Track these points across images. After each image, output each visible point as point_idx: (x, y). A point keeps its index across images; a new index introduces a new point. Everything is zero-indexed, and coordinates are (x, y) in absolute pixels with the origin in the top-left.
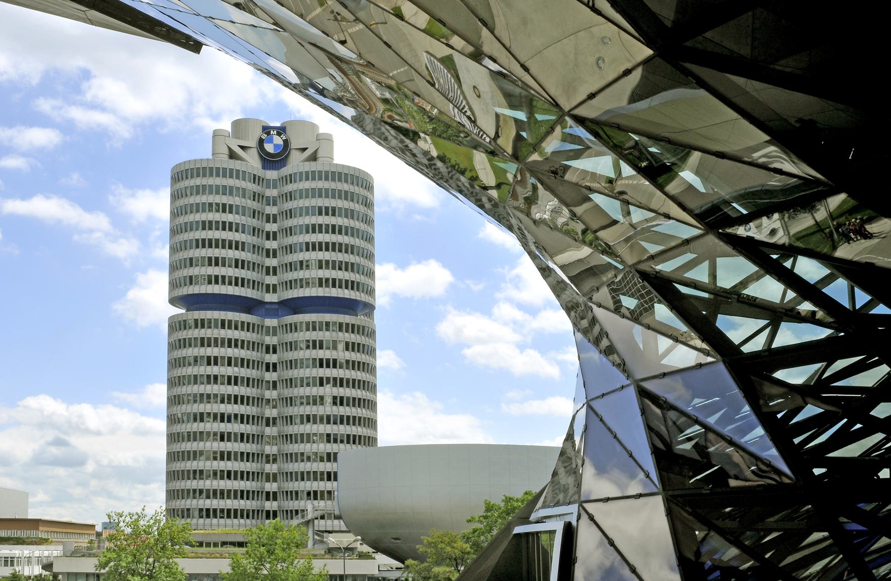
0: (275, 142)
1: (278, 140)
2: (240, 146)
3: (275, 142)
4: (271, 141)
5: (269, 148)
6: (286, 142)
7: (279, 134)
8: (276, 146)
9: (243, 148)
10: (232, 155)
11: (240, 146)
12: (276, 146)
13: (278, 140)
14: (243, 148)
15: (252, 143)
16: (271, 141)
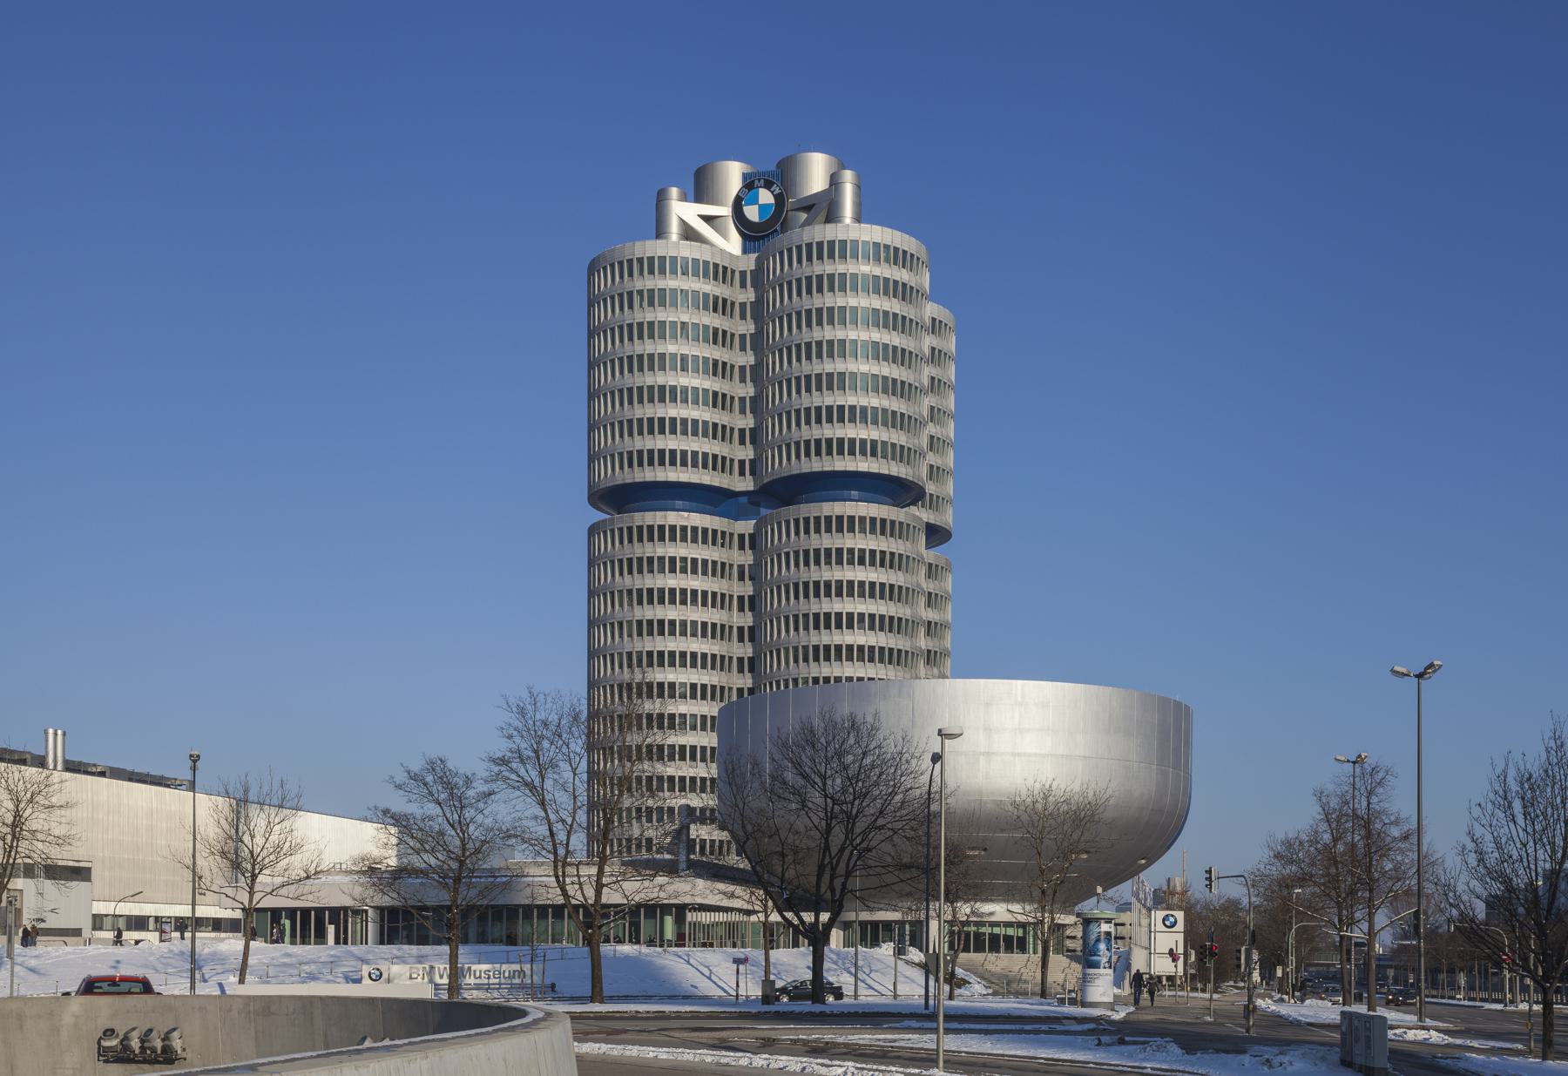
0: (761, 202)
1: (766, 197)
2: (701, 217)
3: (761, 202)
4: (755, 201)
5: (752, 213)
6: (780, 199)
7: (768, 185)
8: (762, 208)
9: (708, 219)
10: (689, 234)
11: (701, 217)
12: (762, 208)
13: (766, 197)
14: (708, 219)
15: (725, 211)
16: (755, 201)
